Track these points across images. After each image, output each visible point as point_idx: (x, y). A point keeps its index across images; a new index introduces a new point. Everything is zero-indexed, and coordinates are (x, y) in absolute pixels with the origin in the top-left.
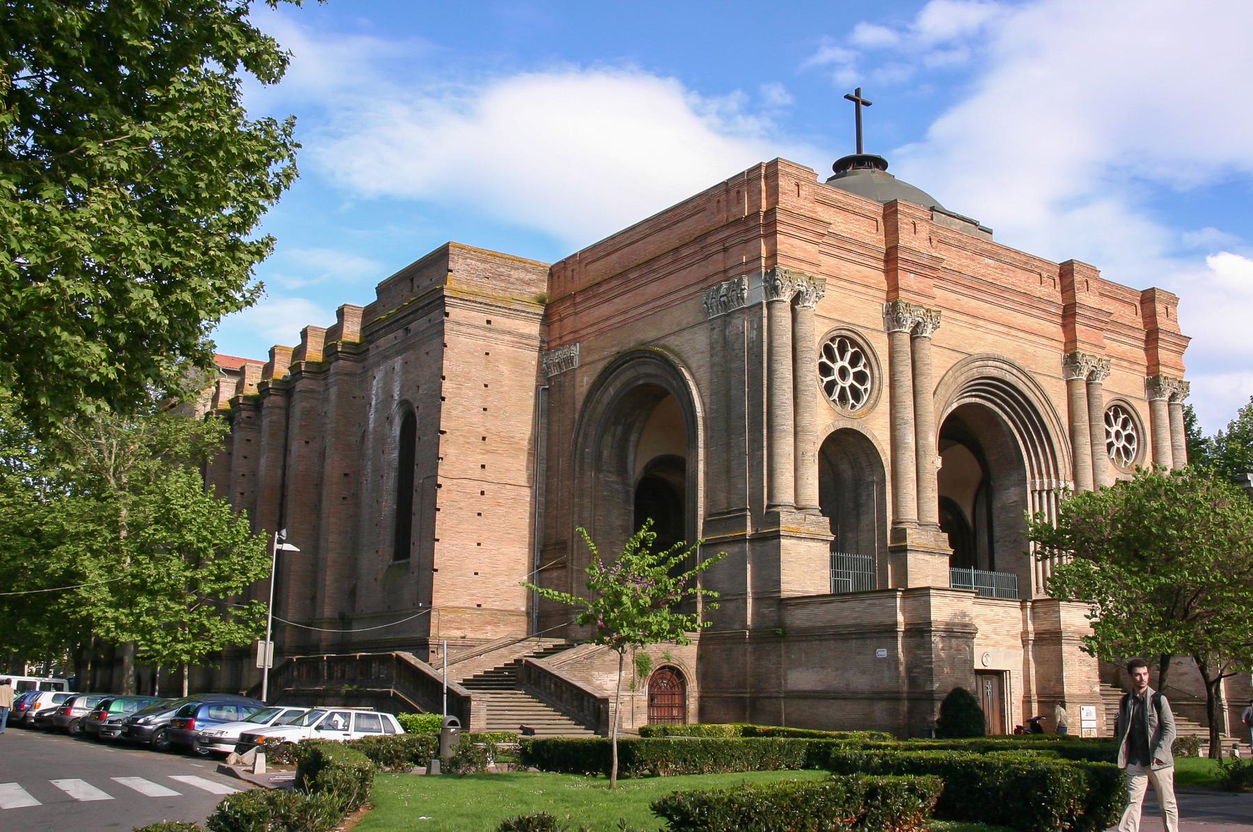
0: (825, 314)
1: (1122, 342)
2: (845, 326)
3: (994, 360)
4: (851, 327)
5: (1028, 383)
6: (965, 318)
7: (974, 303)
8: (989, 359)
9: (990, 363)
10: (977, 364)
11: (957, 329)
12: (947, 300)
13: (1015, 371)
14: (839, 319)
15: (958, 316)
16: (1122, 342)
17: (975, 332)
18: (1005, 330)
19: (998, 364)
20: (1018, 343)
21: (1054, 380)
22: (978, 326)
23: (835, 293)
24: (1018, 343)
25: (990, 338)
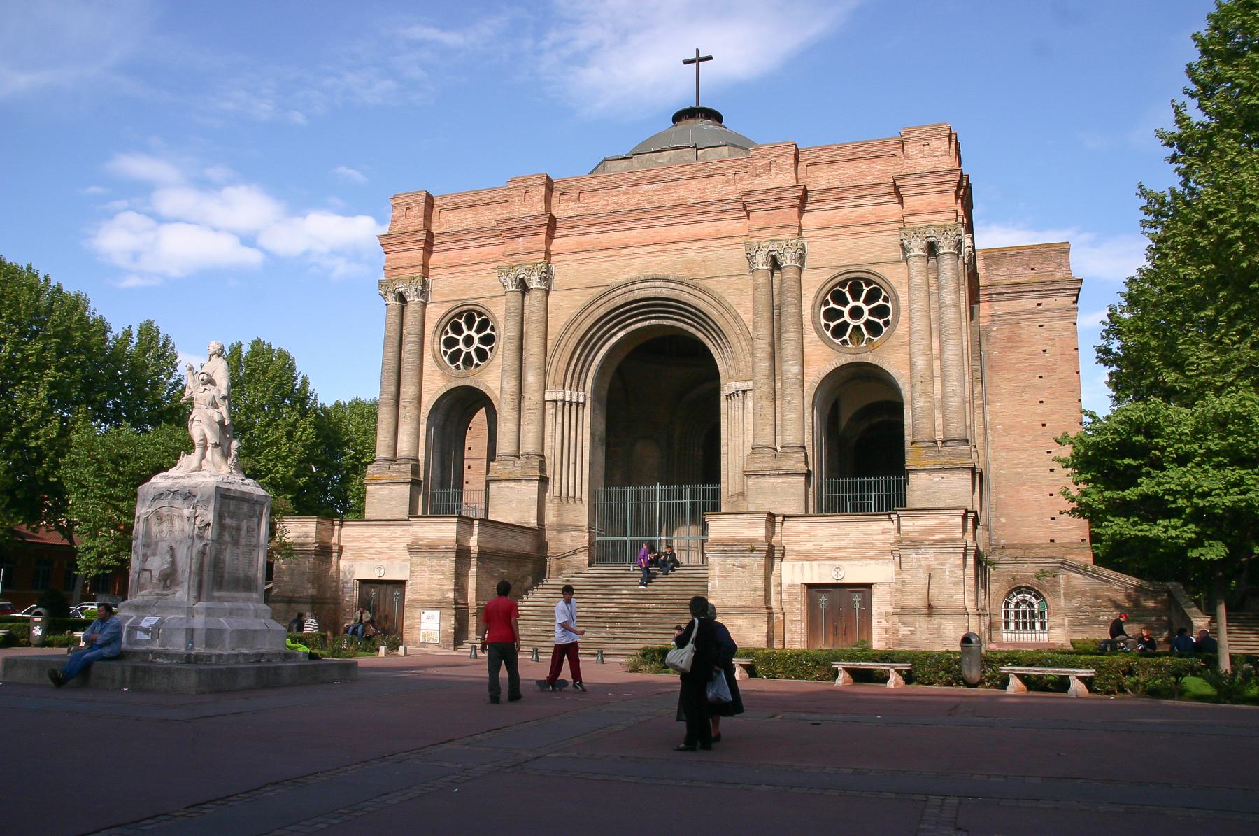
3: (642, 281)
5: (692, 291)
7: (616, 235)
9: (636, 286)
10: (619, 292)
11: (594, 266)
13: (673, 285)
15: (595, 254)
18: (659, 248)
19: (648, 284)
21: (733, 279)
22: (621, 256)
24: (679, 256)
25: (637, 263)
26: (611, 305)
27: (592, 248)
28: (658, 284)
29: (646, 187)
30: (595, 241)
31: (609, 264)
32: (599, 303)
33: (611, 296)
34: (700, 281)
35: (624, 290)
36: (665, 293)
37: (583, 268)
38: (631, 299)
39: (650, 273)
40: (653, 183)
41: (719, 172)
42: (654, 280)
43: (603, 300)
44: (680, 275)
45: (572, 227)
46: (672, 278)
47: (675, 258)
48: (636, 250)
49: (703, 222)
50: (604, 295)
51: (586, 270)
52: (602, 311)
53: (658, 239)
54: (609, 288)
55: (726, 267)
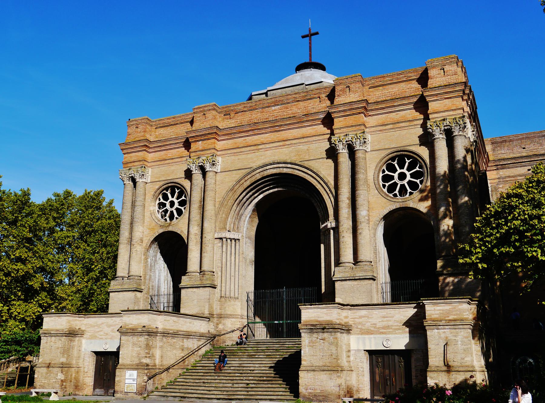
0: (157, 180)
1: (399, 111)
2: (169, 181)
3: (271, 164)
4: (172, 181)
6: (249, 148)
8: (267, 165)
9: (268, 167)
10: (258, 171)
11: (244, 156)
12: (236, 143)
13: (289, 166)
14: (165, 179)
15: (243, 149)
16: (399, 111)
17: (257, 154)
18: (281, 143)
19: (275, 166)
20: (293, 148)
22: (259, 149)
23: (164, 168)
25: (269, 153)
26: (254, 179)
27: (242, 146)
28: (281, 165)
29: (273, 108)
30: (244, 141)
31: (252, 154)
32: (246, 178)
33: (253, 174)
34: (306, 162)
35: (261, 170)
36: (285, 171)
37: (237, 158)
38: (265, 175)
39: (276, 159)
40: (278, 105)
41: (316, 96)
42: (278, 163)
43: (249, 177)
44: (294, 159)
45: (231, 134)
46: (289, 161)
47: (291, 149)
48: (267, 146)
49: (305, 127)
50: (249, 173)
51: (239, 159)
52: (248, 183)
53: (281, 138)
54: (252, 169)
55: (321, 153)
